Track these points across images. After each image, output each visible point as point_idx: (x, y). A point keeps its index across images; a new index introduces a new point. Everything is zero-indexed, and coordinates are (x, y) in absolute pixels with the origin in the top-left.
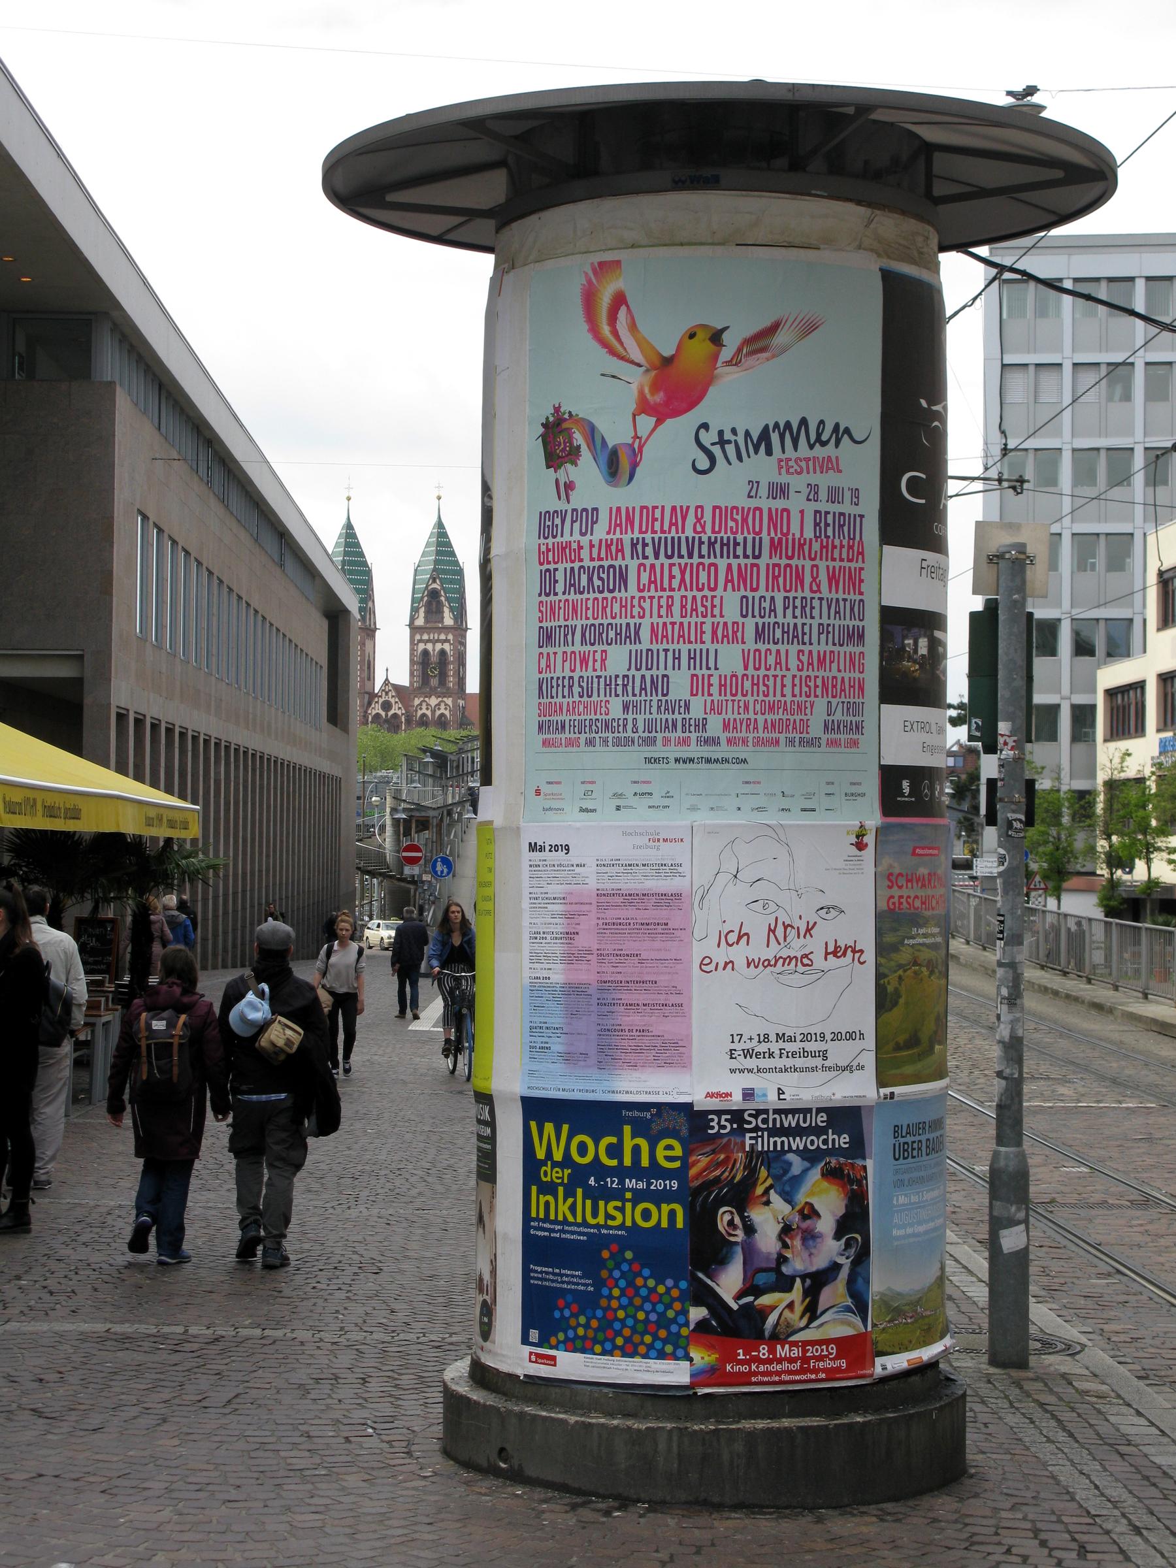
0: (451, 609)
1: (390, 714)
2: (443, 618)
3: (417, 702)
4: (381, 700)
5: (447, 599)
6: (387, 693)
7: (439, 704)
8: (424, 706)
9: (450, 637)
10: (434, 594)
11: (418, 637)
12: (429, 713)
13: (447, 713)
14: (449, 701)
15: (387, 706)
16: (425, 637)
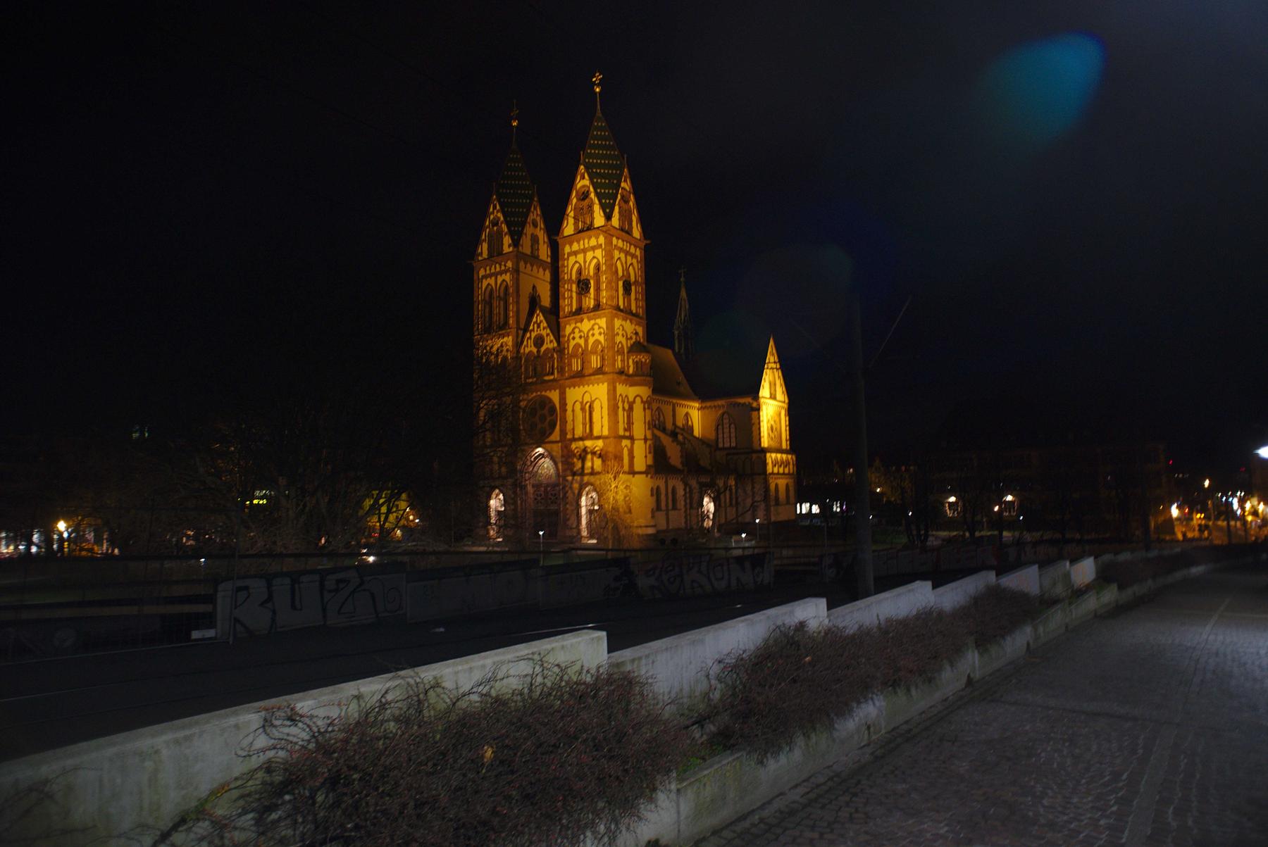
0: (603, 207)
1: (543, 349)
2: (593, 219)
3: (568, 329)
4: (533, 335)
5: (597, 194)
6: (539, 326)
7: (592, 329)
8: (577, 335)
9: (602, 240)
10: (584, 196)
11: (567, 249)
12: (582, 342)
13: (602, 338)
14: (602, 322)
15: (539, 341)
16: (575, 247)
